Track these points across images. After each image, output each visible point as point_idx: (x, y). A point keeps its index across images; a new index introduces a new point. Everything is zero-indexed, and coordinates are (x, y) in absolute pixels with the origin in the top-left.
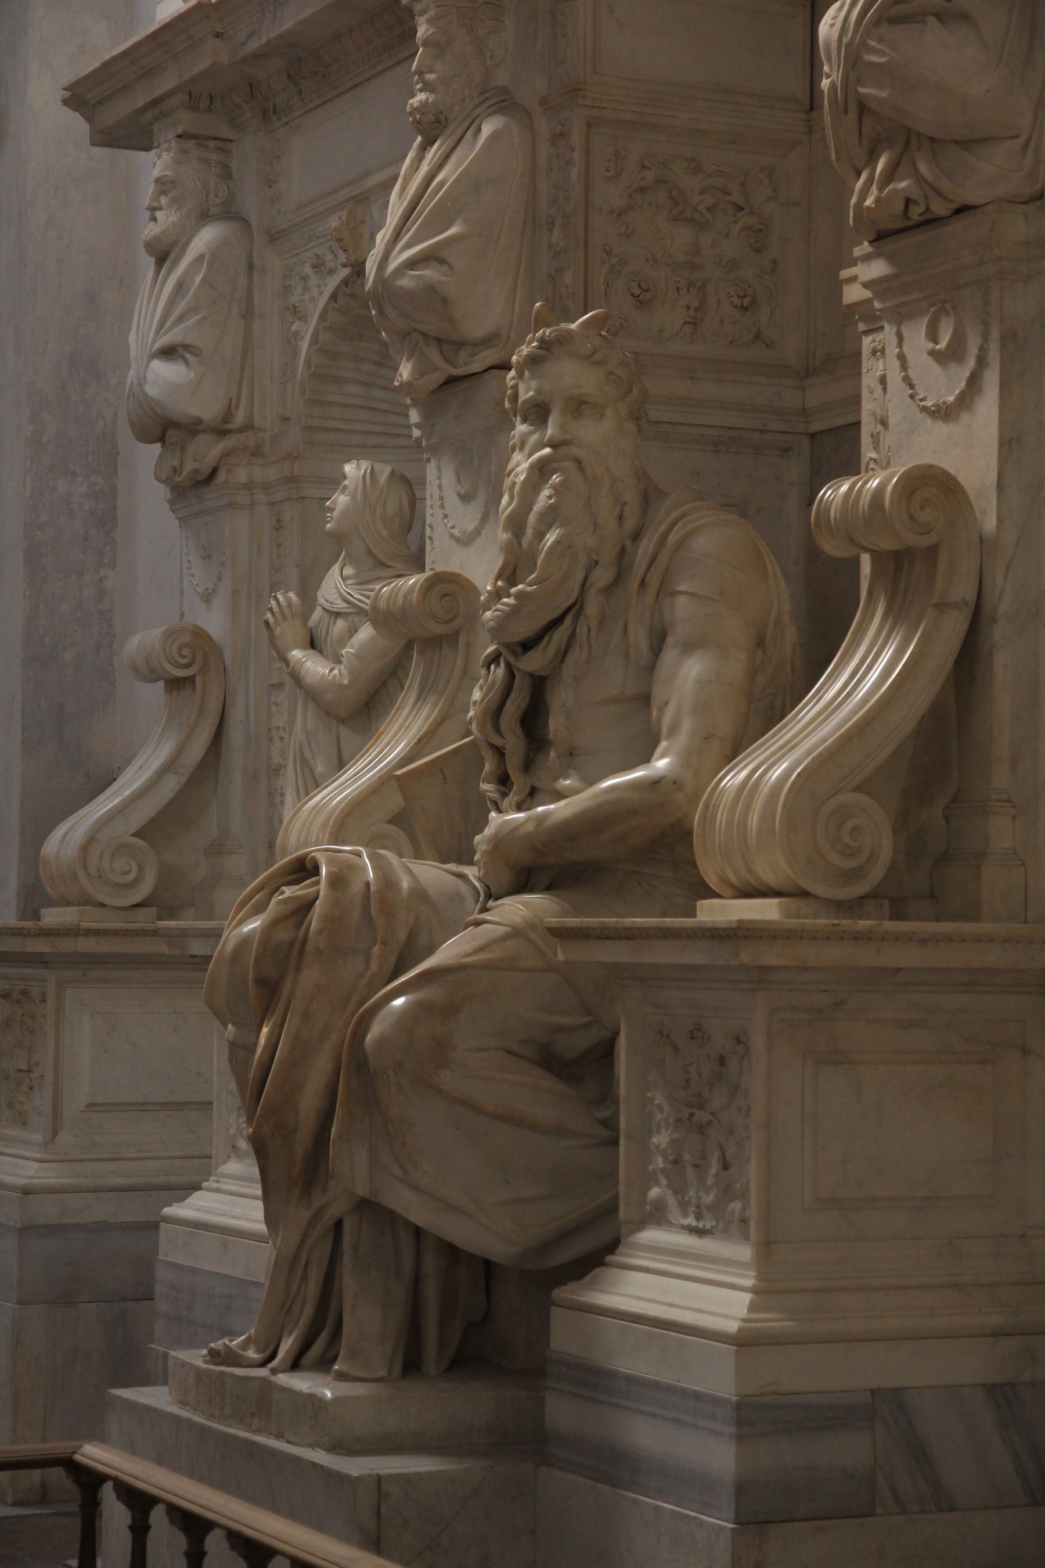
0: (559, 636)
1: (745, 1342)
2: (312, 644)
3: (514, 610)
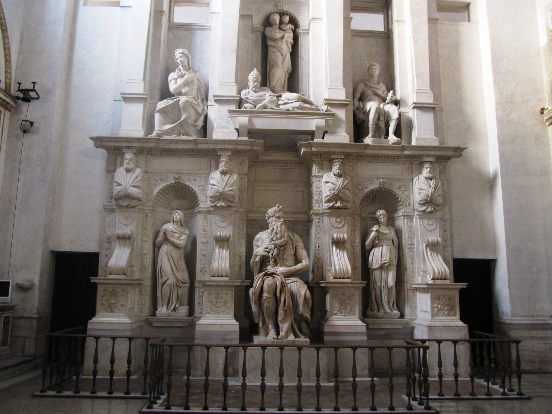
2: (172, 237)
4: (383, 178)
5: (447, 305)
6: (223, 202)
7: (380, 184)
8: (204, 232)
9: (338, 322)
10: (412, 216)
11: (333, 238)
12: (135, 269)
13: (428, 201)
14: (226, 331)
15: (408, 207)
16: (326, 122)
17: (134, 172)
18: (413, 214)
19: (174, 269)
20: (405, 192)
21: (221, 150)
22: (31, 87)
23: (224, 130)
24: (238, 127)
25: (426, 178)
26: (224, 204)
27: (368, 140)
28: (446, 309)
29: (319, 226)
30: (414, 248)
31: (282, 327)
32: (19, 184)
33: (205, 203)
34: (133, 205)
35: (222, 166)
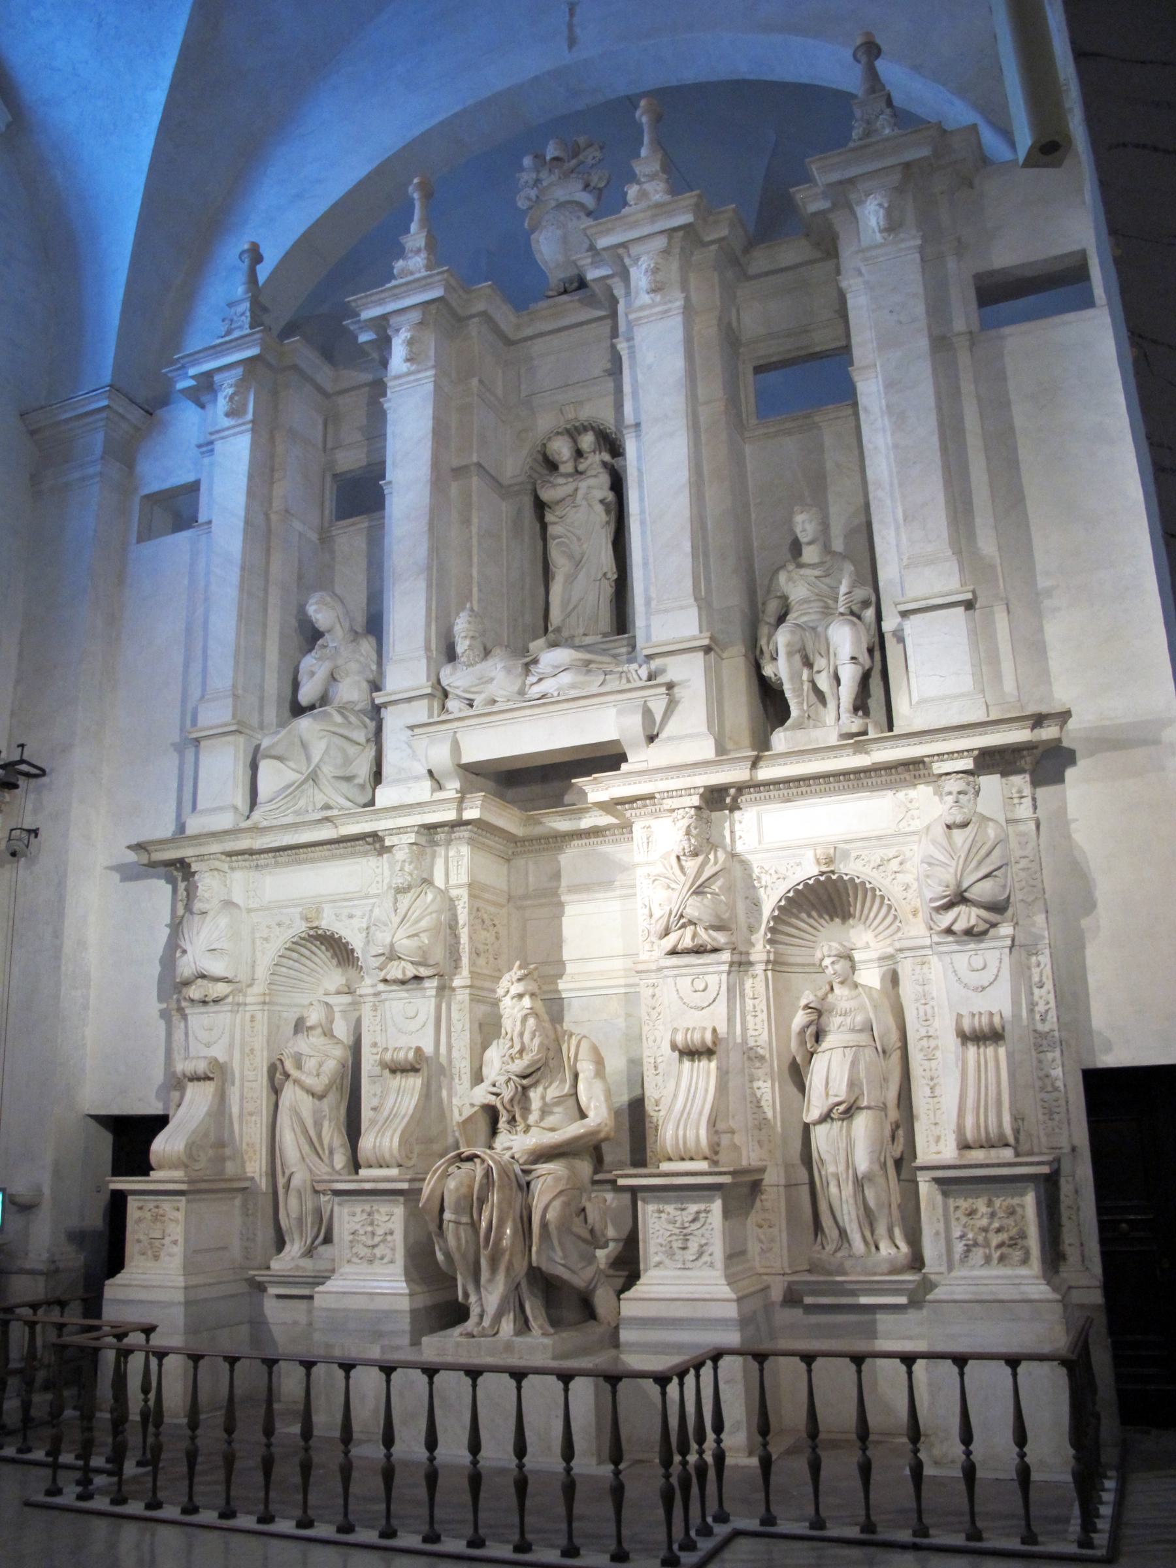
5: (998, 1231)
8: (375, 1051)
10: (923, 948)
12: (228, 1151)
14: (377, 1311)
16: (647, 713)
19: (306, 1148)
22: (16, 757)
25: (949, 827)
27: (780, 739)
28: (994, 1243)
30: (936, 1048)
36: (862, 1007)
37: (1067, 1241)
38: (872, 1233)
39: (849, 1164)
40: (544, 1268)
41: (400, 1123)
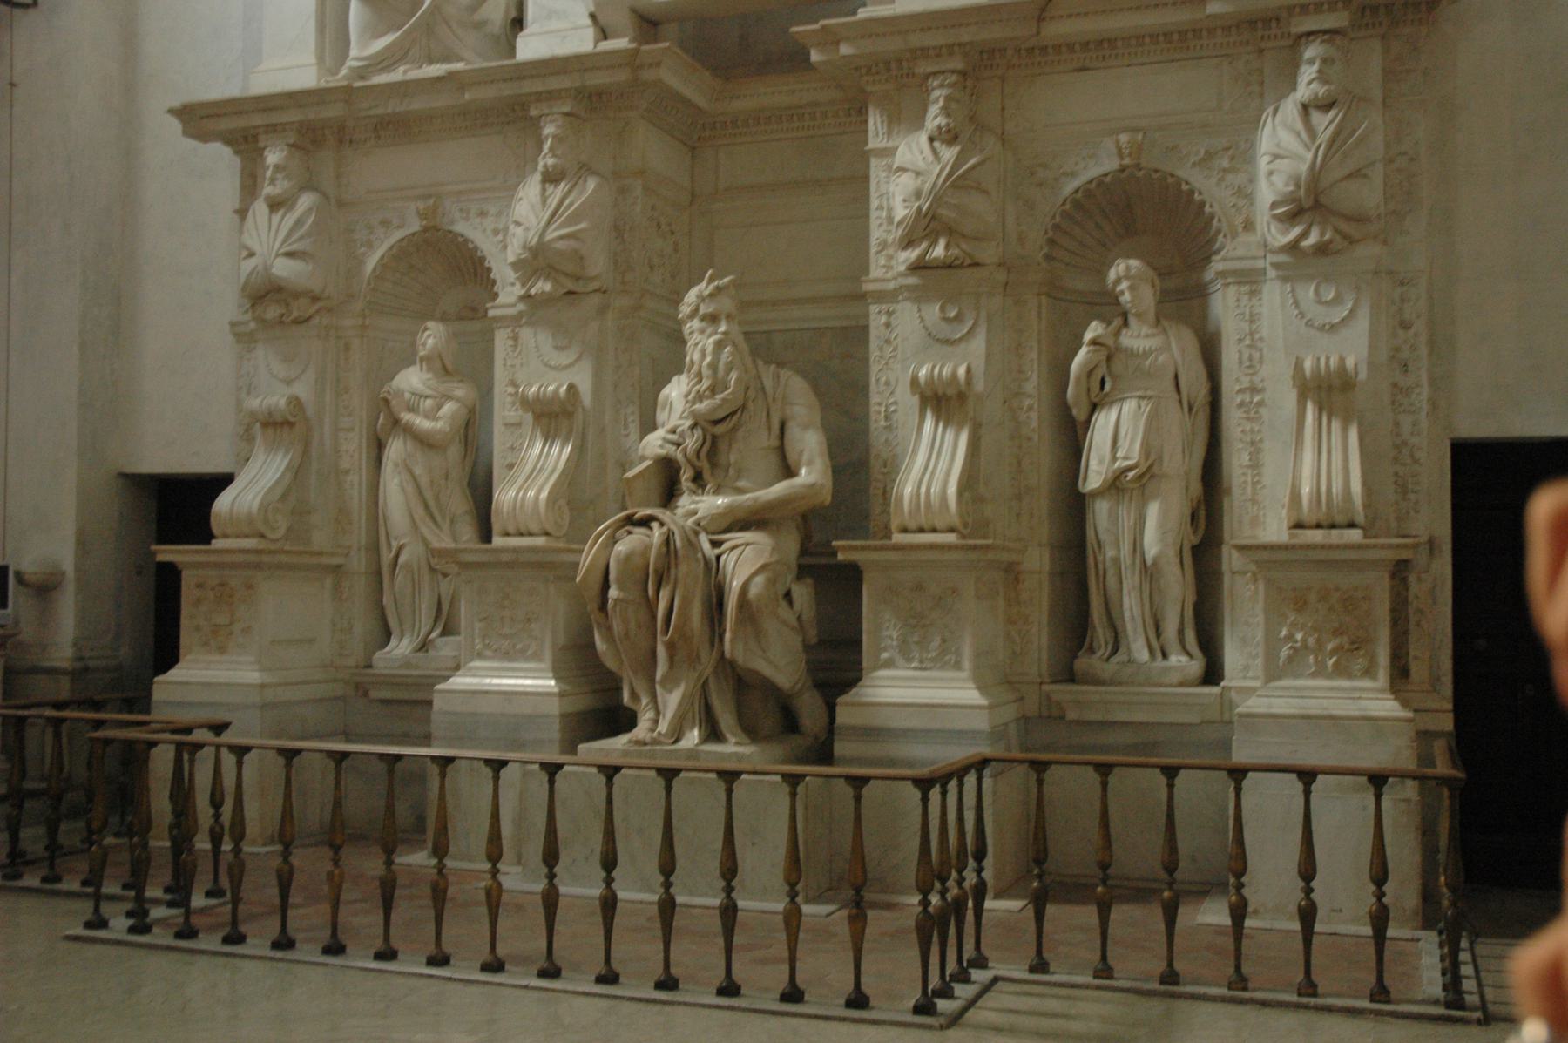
0: (735, 418)
1: (991, 707)
2: (412, 409)
3: (720, 406)
4: (1135, 130)
5: (1337, 632)
6: (547, 278)
7: (1121, 155)
8: (511, 390)
9: (888, 691)
11: (914, 381)
13: (1306, 204)
15: (1243, 238)
17: (292, 207)
18: (1260, 264)
19: (420, 512)
20: (1230, 177)
21: (539, 97)
23: (554, 25)
24: (592, 9)
26: (548, 287)
28: (1330, 647)
29: (888, 342)
30: (1260, 404)
31: (665, 703)
32: (14, 279)
33: (509, 293)
34: (295, 314)
35: (547, 160)
36: (1167, 347)
37: (1412, 653)
38: (1158, 636)
39: (1137, 546)
40: (740, 660)
41: (548, 479)
